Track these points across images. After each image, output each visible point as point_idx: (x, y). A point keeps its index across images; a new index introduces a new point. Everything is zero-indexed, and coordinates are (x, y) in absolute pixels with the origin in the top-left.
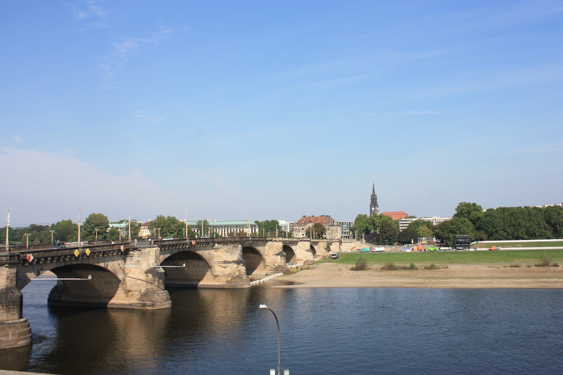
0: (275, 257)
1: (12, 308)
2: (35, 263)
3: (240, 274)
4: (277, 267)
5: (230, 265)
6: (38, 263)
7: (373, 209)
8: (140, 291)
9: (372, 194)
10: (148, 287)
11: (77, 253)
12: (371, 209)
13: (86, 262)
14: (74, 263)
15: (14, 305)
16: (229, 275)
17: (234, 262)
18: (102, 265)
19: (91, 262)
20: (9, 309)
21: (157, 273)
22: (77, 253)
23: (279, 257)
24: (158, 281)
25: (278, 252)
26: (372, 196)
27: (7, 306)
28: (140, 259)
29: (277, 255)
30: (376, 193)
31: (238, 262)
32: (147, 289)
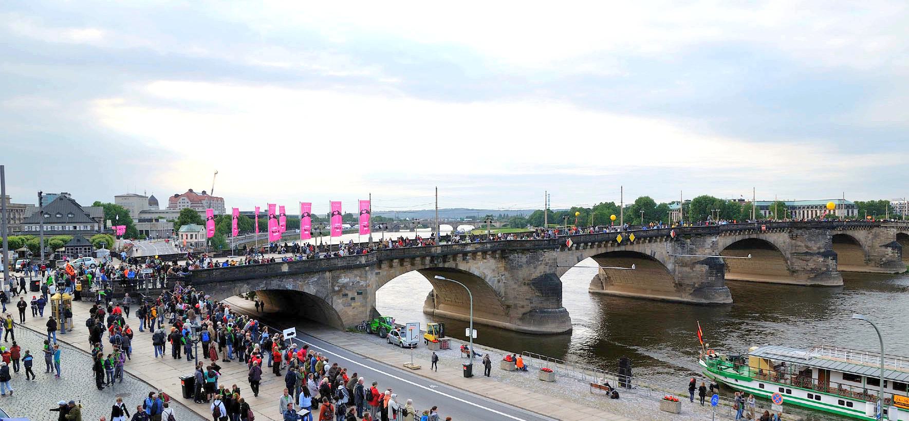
0: (883, 249)
2: (574, 248)
4: (885, 264)
5: (815, 258)
6: (577, 248)
11: (619, 239)
13: (629, 248)
14: (616, 249)
18: (648, 252)
19: (636, 248)
21: (716, 265)
22: (619, 239)
23: (890, 249)
25: (888, 242)
29: (887, 246)
31: (825, 255)
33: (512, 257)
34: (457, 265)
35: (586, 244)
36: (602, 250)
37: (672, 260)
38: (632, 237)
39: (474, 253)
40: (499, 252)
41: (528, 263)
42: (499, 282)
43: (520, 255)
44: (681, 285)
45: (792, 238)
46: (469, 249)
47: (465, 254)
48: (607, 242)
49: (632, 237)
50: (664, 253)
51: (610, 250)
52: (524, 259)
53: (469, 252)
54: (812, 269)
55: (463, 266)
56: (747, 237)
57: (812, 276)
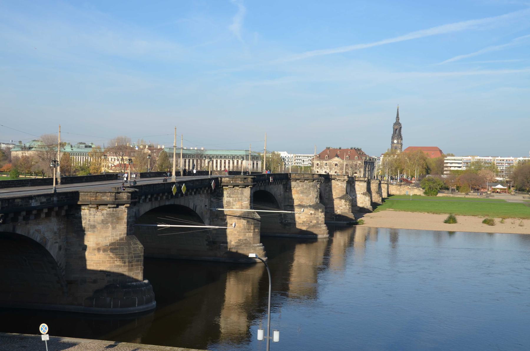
1: (137, 265)
7: (395, 141)
9: (395, 121)
10: (241, 238)
12: (393, 143)
15: (138, 261)
17: (310, 206)
18: (191, 206)
19: (182, 202)
20: (132, 266)
24: (254, 229)
26: (395, 124)
27: (129, 262)
28: (231, 199)
30: (400, 121)
32: (240, 240)
35: (146, 198)
36: (156, 205)
37: (208, 215)
39: (39, 210)
40: (66, 208)
42: (60, 248)
43: (93, 211)
44: (214, 243)
46: (34, 203)
47: (29, 211)
48: (163, 194)
50: (203, 206)
51: (162, 204)
53: (35, 208)
54: (304, 222)
56: (258, 189)
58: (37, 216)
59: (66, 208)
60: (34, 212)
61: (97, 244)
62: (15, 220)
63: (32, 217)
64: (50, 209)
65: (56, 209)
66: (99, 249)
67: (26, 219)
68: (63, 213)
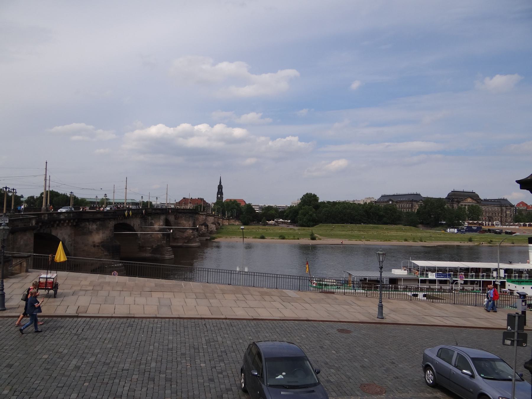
3: (194, 238)
8: (152, 247)
16: (186, 238)
18: (132, 225)
19: (128, 221)
23: (203, 227)
29: (202, 225)
32: (158, 245)
33: (83, 225)
34: (51, 231)
38: (131, 213)
39: (64, 220)
41: (98, 230)
42: (71, 245)
45: (175, 219)
46: (62, 217)
47: (60, 220)
49: (131, 213)
52: (95, 227)
53: (62, 219)
55: (54, 233)
57: (186, 241)
58: (63, 224)
59: (76, 220)
60: (62, 222)
61: (94, 242)
62: (53, 226)
63: (60, 224)
64: (69, 221)
65: (72, 221)
66: (94, 246)
67: (58, 225)
68: (75, 224)
